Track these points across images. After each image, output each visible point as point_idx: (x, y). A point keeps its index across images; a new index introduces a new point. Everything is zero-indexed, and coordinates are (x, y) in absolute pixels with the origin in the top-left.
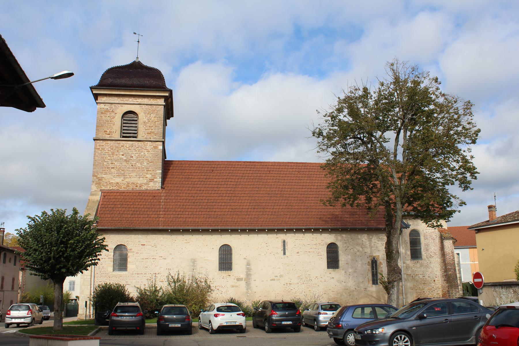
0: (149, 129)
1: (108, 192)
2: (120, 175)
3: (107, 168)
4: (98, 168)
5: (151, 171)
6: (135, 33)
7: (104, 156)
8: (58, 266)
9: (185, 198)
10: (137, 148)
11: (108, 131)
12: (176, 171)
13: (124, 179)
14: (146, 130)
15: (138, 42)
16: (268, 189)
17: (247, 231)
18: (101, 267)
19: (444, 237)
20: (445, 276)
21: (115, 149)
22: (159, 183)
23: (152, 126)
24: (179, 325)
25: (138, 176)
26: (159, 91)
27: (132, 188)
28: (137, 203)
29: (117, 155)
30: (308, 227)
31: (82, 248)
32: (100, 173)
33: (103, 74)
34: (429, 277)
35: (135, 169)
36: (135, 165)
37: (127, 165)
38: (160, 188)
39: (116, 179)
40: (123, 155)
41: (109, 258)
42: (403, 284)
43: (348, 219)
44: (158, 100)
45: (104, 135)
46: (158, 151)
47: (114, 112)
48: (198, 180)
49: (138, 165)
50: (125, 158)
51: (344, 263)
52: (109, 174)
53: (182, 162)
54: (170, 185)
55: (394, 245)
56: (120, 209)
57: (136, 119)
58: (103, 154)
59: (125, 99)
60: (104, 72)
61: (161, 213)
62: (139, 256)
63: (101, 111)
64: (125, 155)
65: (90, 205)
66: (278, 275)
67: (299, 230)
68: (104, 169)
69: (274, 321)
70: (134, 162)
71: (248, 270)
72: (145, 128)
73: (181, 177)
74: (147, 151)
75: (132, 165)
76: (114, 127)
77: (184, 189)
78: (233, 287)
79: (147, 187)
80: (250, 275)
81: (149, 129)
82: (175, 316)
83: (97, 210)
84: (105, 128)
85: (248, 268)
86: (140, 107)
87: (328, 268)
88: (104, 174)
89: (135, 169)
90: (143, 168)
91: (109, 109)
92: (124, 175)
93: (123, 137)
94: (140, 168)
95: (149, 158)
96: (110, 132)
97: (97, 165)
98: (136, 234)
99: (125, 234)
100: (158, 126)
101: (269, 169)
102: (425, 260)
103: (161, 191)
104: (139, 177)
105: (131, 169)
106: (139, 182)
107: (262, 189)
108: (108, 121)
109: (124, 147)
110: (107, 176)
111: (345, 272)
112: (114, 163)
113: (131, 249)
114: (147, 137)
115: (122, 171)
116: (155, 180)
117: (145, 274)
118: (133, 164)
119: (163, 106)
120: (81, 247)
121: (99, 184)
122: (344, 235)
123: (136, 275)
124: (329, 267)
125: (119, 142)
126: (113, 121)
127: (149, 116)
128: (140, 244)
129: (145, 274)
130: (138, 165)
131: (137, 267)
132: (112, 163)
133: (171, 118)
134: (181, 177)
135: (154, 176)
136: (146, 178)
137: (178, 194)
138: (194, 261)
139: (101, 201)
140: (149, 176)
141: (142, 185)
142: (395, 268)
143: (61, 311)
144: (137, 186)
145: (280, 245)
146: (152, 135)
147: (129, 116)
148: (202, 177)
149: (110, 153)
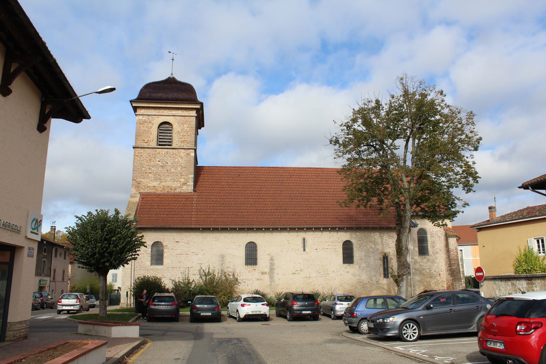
0: (183, 138)
1: (146, 194)
2: (157, 179)
3: (145, 173)
4: (138, 173)
5: (184, 175)
6: (170, 52)
7: (142, 162)
8: (102, 261)
9: (215, 200)
10: (172, 155)
11: (146, 140)
12: (206, 175)
13: (161, 183)
14: (179, 138)
15: (173, 60)
16: (290, 192)
17: (271, 229)
18: (140, 262)
19: (449, 235)
20: (450, 270)
21: (152, 156)
22: (191, 186)
23: (185, 136)
24: (210, 314)
25: (173, 180)
26: (191, 103)
27: (168, 191)
28: (172, 205)
29: (153, 161)
30: (325, 226)
31: (123, 244)
32: (139, 177)
33: (141, 88)
34: (434, 271)
35: (170, 174)
36: (170, 171)
37: (162, 170)
38: (192, 191)
39: (153, 183)
40: (159, 161)
41: (147, 254)
42: (412, 277)
43: (362, 219)
44: (190, 111)
45: (142, 144)
46: (190, 158)
47: (151, 123)
48: (226, 184)
49: (173, 170)
50: (161, 164)
51: (358, 259)
52: (147, 178)
53: (212, 167)
54: (201, 188)
55: (403, 242)
56: (157, 210)
57: (171, 129)
58: (142, 161)
59: (161, 112)
60: (142, 87)
61: (193, 213)
62: (173, 252)
64: (161, 162)
65: (130, 206)
66: (299, 269)
67: (317, 229)
68: (142, 174)
69: (295, 311)
70: (169, 168)
71: (272, 264)
72: (179, 137)
73: (211, 181)
74: (180, 158)
76: (151, 136)
77: (214, 192)
78: (258, 280)
79: (181, 190)
80: (273, 269)
81: (183, 138)
82: (206, 306)
83: (137, 210)
85: (272, 263)
86: (174, 118)
87: (343, 263)
88: (143, 179)
89: (170, 174)
90: (177, 173)
92: (160, 179)
93: (160, 145)
94: (174, 173)
95: (182, 164)
96: (147, 140)
97: (137, 170)
98: (171, 232)
99: (161, 232)
100: (191, 135)
101: (291, 174)
102: (431, 256)
103: (193, 194)
104: (173, 181)
105: (167, 174)
106: (173, 186)
107: (285, 192)
108: (146, 131)
110: (145, 180)
111: (359, 267)
112: (151, 168)
113: (166, 246)
114: (181, 145)
115: (158, 175)
116: (188, 183)
117: (179, 268)
118: (168, 170)
119: (195, 118)
120: (123, 243)
122: (358, 234)
123: (171, 269)
124: (344, 262)
125: (155, 150)
126: (150, 131)
129: (179, 268)
130: (173, 170)
133: (202, 128)
134: (211, 181)
136: (179, 182)
137: (208, 197)
138: (223, 257)
139: (140, 202)
140: (182, 180)
141: (176, 188)
142: (405, 263)
143: (105, 300)
144: (171, 189)
145: (301, 242)
146: (185, 143)
147: (165, 126)
148: (230, 181)
149: (148, 160)
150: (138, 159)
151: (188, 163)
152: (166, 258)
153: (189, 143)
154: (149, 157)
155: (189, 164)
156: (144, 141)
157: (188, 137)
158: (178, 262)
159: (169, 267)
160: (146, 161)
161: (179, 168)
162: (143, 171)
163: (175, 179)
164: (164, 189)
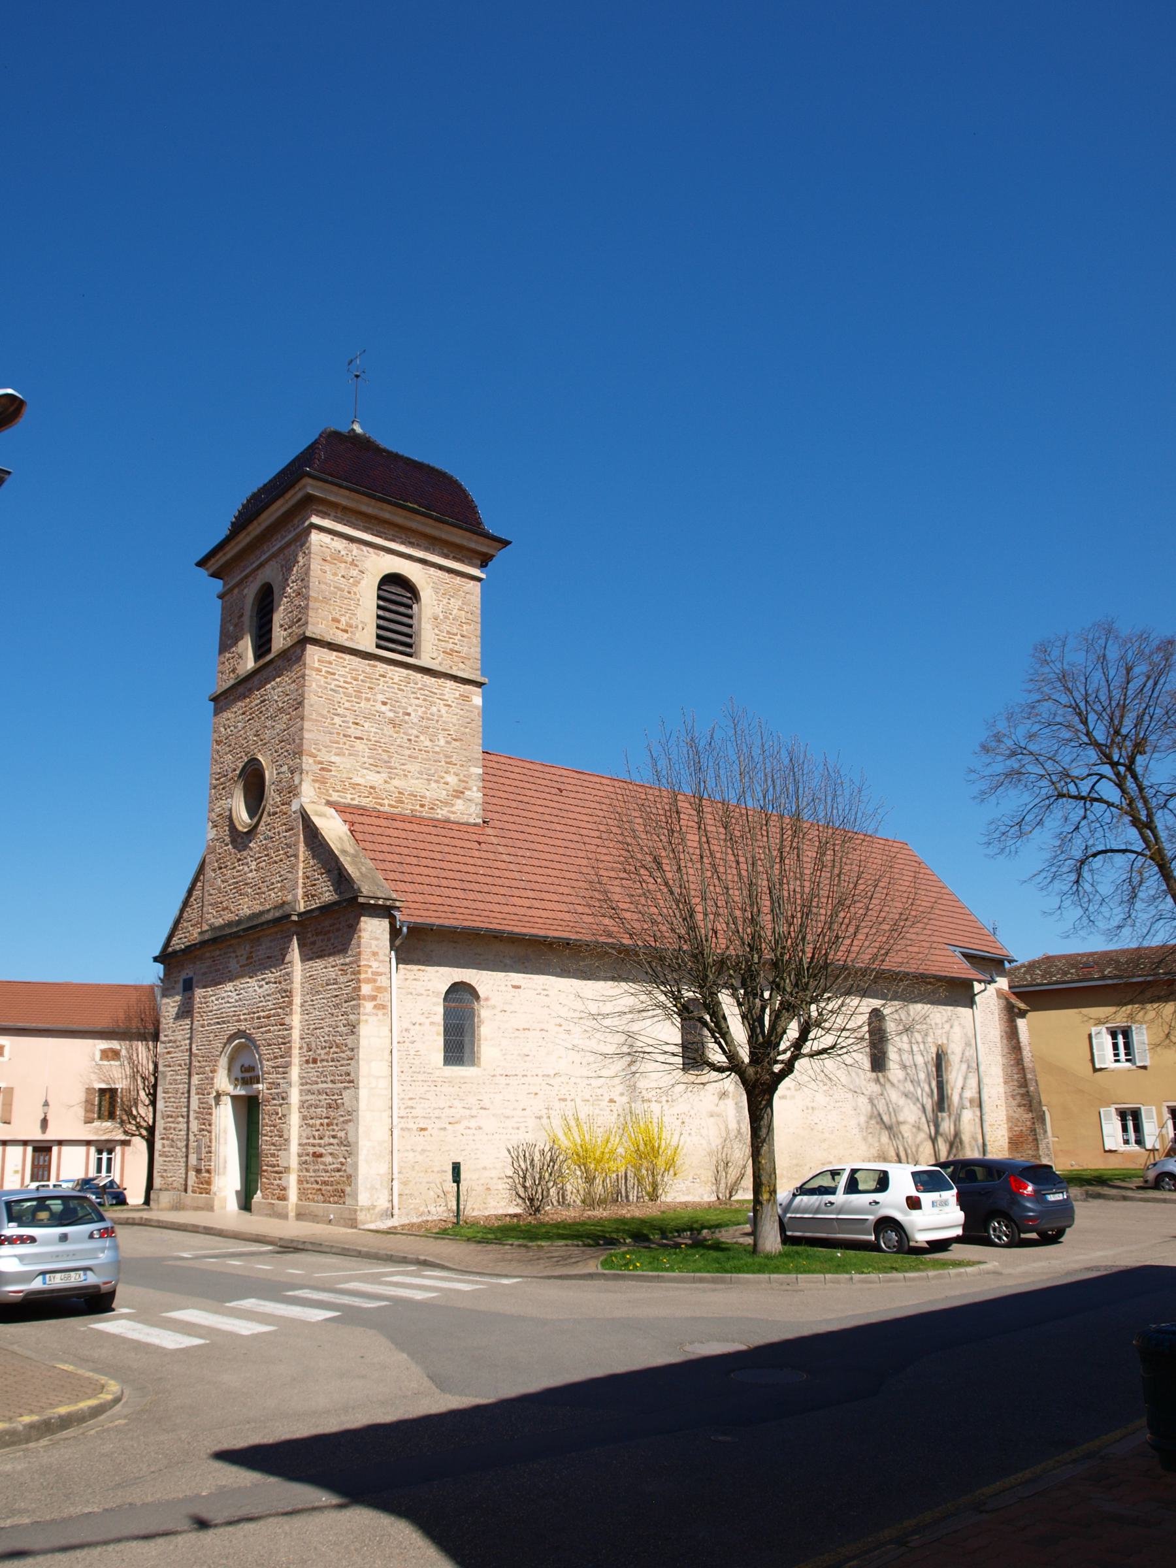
3: (344, 735)
5: (456, 764)
7: (334, 697)
10: (421, 689)
11: (343, 619)
13: (391, 778)
14: (439, 640)
18: (412, 1052)
20: (1022, 1095)
21: (362, 681)
22: (476, 805)
23: (454, 635)
29: (368, 700)
35: (417, 752)
36: (416, 742)
37: (395, 735)
38: (480, 821)
40: (384, 703)
41: (432, 1023)
45: (331, 632)
46: (472, 712)
47: (356, 566)
50: (391, 715)
52: (350, 755)
63: (322, 552)
64: (388, 707)
75: (410, 740)
78: (712, 1116)
79: (448, 811)
84: (334, 609)
88: (337, 754)
90: (436, 753)
91: (343, 553)
104: (428, 780)
105: (408, 752)
106: (428, 794)
109: (387, 679)
110: (344, 759)
112: (361, 722)
113: (487, 999)
115: (384, 751)
116: (467, 793)
117: (523, 1076)
118: (412, 738)
121: (323, 782)
123: (503, 1080)
126: (355, 594)
127: (445, 601)
128: (509, 984)
129: (523, 1076)
131: (504, 1055)
132: (357, 724)
135: (464, 781)
140: (452, 779)
141: (435, 805)
144: (422, 806)
146: (456, 659)
150: (319, 681)
151: (466, 727)
152: (486, 1040)
153: (466, 661)
154: (355, 683)
155: (467, 730)
156: (337, 624)
157: (463, 641)
158: (519, 1055)
159: (495, 1073)
160: (344, 693)
161: (440, 736)
162: (337, 726)
163: (433, 772)
164: (402, 802)
